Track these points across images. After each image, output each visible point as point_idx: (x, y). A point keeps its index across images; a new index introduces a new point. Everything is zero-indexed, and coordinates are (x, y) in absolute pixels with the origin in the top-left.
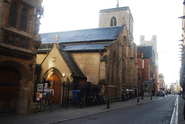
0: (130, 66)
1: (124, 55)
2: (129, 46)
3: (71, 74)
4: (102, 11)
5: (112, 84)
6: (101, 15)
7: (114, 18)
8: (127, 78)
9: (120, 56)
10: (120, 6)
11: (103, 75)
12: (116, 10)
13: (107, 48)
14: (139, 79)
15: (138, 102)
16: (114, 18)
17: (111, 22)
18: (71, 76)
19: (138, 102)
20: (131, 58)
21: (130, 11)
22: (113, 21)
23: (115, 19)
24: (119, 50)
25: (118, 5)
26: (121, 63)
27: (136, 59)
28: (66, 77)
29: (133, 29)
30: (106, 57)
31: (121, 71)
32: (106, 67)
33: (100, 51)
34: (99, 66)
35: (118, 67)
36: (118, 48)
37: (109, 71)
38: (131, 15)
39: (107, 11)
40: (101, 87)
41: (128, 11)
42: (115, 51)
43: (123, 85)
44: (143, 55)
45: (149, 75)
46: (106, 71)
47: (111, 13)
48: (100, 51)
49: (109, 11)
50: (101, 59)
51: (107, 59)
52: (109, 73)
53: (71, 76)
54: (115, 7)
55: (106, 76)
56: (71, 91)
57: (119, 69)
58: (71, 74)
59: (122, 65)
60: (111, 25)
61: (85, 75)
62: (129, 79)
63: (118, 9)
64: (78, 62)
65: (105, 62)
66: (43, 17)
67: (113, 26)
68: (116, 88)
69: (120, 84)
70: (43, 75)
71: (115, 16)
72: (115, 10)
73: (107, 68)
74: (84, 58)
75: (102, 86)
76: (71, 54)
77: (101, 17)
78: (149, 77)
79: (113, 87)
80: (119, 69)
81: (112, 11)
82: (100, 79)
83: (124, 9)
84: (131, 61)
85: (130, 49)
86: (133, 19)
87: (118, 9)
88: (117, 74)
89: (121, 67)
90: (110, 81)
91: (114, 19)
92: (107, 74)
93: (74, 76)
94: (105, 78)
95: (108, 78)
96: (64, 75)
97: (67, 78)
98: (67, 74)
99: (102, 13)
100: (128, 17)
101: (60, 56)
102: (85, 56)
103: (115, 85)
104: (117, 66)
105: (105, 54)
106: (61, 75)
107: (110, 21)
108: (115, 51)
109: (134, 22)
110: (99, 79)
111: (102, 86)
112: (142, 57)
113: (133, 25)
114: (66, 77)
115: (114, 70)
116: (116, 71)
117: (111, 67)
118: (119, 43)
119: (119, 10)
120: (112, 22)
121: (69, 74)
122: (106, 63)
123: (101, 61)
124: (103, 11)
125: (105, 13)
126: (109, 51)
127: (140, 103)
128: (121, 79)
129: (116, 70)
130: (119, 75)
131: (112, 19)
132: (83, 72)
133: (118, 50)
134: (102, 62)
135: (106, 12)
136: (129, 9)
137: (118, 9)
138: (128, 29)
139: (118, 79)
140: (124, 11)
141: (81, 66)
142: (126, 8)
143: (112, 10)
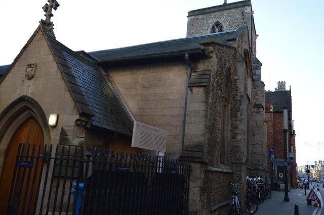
0: (253, 123)
3: (78, 117)
4: (192, 14)
5: (223, 163)
6: (191, 20)
7: (218, 25)
11: (196, 131)
13: (211, 48)
20: (258, 106)
24: (239, 74)
30: (204, 74)
31: (243, 127)
32: (206, 102)
33: (187, 55)
34: (183, 105)
35: (236, 116)
37: (216, 119)
38: (252, 17)
39: (204, 12)
40: (190, 170)
41: (248, 10)
43: (247, 168)
46: (206, 116)
48: (187, 55)
49: (207, 11)
50: (192, 80)
51: (209, 79)
53: (78, 123)
54: (222, 3)
55: (207, 135)
56: (68, 184)
57: (238, 123)
58: (78, 117)
59: (247, 111)
60: (213, 30)
62: (253, 153)
63: (227, 7)
64: (122, 93)
68: (232, 174)
69: (243, 164)
71: (221, 20)
72: (216, 9)
73: (210, 108)
74: (140, 81)
75: (193, 165)
76: (107, 72)
77: (190, 25)
79: (225, 171)
80: (238, 123)
81: (214, 12)
82: (186, 143)
83: (240, 5)
84: (257, 113)
88: (234, 136)
90: (217, 153)
91: (217, 27)
92: (211, 128)
94: (202, 139)
95: (212, 143)
96: (52, 120)
97: (63, 133)
99: (193, 17)
101: (51, 57)
102: (143, 76)
103: (227, 165)
104: (234, 115)
105: (201, 67)
106: (45, 121)
110: (183, 144)
111: (193, 165)
112: (271, 110)
113: (255, 43)
114: (59, 128)
115: (226, 123)
116: (230, 127)
118: (238, 54)
122: (207, 93)
123: (191, 86)
124: (196, 13)
125: (200, 17)
129: (230, 123)
130: (239, 137)
131: (213, 28)
134: (195, 90)
139: (235, 149)
143: (214, 10)
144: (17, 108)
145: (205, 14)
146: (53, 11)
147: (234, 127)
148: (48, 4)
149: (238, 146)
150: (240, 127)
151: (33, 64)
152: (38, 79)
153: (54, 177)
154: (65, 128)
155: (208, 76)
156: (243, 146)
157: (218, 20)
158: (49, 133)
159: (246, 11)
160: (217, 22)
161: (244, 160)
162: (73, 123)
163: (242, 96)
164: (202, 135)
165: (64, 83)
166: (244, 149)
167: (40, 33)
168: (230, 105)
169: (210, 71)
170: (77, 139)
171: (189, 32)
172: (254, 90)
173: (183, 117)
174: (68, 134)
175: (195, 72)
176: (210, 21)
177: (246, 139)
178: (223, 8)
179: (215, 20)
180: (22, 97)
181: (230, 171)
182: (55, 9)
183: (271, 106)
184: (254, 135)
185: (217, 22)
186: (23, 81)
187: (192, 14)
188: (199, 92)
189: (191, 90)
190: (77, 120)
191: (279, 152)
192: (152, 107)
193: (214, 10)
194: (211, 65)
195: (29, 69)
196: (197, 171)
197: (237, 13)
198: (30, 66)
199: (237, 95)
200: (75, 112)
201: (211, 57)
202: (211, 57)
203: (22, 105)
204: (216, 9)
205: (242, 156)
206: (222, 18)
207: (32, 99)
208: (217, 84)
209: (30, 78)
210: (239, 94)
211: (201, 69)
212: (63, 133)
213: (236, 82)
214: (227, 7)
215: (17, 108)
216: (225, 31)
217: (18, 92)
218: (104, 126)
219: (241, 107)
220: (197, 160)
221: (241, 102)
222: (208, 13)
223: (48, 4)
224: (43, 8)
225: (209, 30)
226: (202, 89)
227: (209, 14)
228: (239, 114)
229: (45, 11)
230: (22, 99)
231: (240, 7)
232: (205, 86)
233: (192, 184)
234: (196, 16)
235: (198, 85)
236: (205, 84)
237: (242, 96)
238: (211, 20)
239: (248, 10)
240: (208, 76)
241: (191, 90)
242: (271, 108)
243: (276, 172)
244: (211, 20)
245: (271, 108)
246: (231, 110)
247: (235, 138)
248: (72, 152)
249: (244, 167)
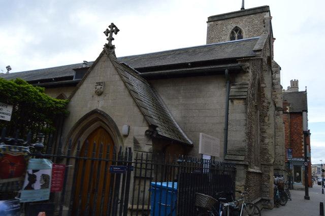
3: (147, 128)
4: (214, 20)
6: (210, 25)
7: (237, 29)
10: (246, 7)
11: (238, 137)
12: (239, 14)
13: (248, 64)
16: (237, 29)
18: (146, 135)
22: (236, 35)
23: (240, 32)
28: (131, 137)
32: (246, 112)
33: (226, 71)
34: (223, 113)
35: (264, 121)
38: (270, 21)
39: (223, 18)
40: (234, 172)
41: (266, 15)
44: (290, 108)
47: (231, 21)
48: (226, 71)
49: (227, 17)
54: (239, 9)
55: (247, 141)
56: (142, 183)
57: (265, 127)
58: (147, 128)
61: (186, 137)
70: (70, 129)
73: (249, 116)
76: (150, 84)
77: (210, 30)
79: (258, 171)
83: (259, 11)
87: (243, 13)
91: (237, 32)
92: (249, 135)
93: (155, 136)
94: (244, 145)
95: (250, 145)
97: (136, 142)
99: (212, 23)
104: (262, 121)
105: (241, 80)
109: (275, 41)
111: (237, 167)
116: (259, 132)
119: (249, 15)
121: (140, 130)
122: (246, 104)
123: (231, 99)
124: (216, 19)
125: (220, 22)
126: (250, 74)
130: (267, 141)
131: (232, 33)
132: (180, 129)
133: (263, 79)
134: (236, 102)
136: (269, 11)
137: (242, 14)
139: (264, 151)
140: (258, 15)
141: (175, 114)
142: (265, 9)
144: (90, 119)
145: (223, 19)
146: (114, 35)
147: (263, 131)
148: (109, 29)
149: (266, 149)
150: (267, 131)
151: (102, 83)
152: (107, 95)
153: (135, 178)
154: (136, 137)
155: (246, 90)
157: (238, 26)
158: (122, 141)
159: (265, 17)
160: (236, 27)
161: (272, 161)
162: (144, 133)
163: (269, 103)
164: (243, 141)
165: (132, 99)
166: (271, 152)
167: (105, 55)
168: (259, 111)
169: (248, 84)
170: (147, 147)
172: (274, 93)
173: (223, 126)
174: (140, 142)
175: (233, 85)
176: (229, 27)
177: (274, 142)
178: (242, 14)
180: (93, 111)
181: (260, 171)
182: (116, 34)
183: (287, 107)
185: (236, 27)
186: (93, 96)
187: (211, 20)
188: (238, 105)
189: (232, 102)
190: (147, 131)
191: (296, 152)
192: (195, 115)
194: (248, 78)
195: (99, 87)
196: (241, 173)
197: (256, 19)
198: (99, 84)
199: (264, 101)
200: (145, 124)
201: (248, 72)
202: (248, 72)
203: (94, 116)
204: (235, 15)
205: (270, 158)
206: (242, 23)
207: (103, 112)
208: (252, 96)
209: (99, 94)
210: (266, 101)
211: (240, 83)
212: (136, 142)
213: (263, 90)
214: (246, 13)
215: (90, 119)
217: (89, 106)
218: (164, 135)
219: (269, 113)
220: (241, 163)
221: (268, 109)
222: (228, 18)
223: (109, 29)
224: (104, 32)
225: (228, 36)
226: (242, 101)
227: (229, 20)
228: (266, 119)
229: (107, 35)
230: (95, 112)
231: (259, 13)
232: (244, 99)
233: (237, 183)
234: (216, 23)
235: (238, 97)
236: (245, 97)
237: (269, 103)
238: (231, 25)
240: (246, 90)
241: (232, 102)
242: (287, 109)
243: (293, 171)
244: (231, 25)
245: (287, 109)
246: (260, 116)
247: (262, 141)
248: (144, 157)
249: (272, 168)
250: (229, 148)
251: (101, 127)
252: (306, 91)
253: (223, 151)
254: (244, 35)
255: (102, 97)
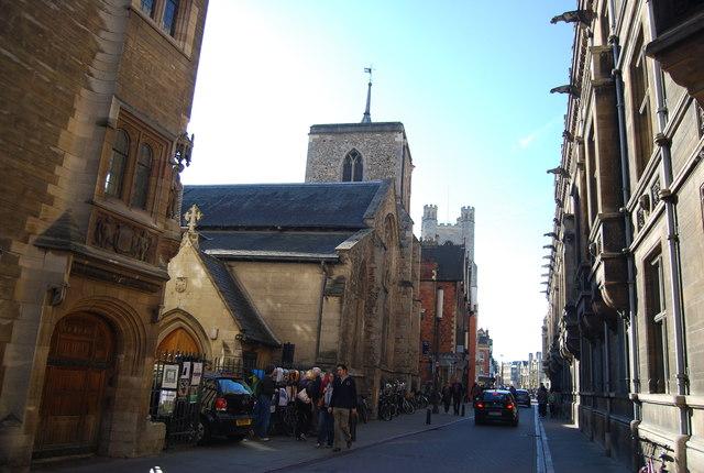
1: (386, 275)
2: (401, 246)
3: (238, 332)
4: (317, 130)
7: (354, 153)
8: (391, 346)
9: (378, 277)
10: (377, 117)
14: (425, 348)
15: (428, 422)
16: (354, 153)
17: (345, 166)
19: (428, 422)
20: (406, 284)
21: (405, 137)
23: (360, 159)
25: (367, 114)
26: (380, 301)
27: (417, 284)
29: (409, 191)
30: (340, 281)
31: (378, 325)
34: (317, 311)
36: (372, 253)
38: (406, 147)
41: (399, 138)
42: (364, 262)
45: (454, 337)
52: (346, 332)
54: (358, 119)
58: (238, 332)
60: (346, 177)
63: (369, 128)
65: (337, 299)
66: (188, 165)
67: (352, 182)
71: (360, 148)
72: (358, 129)
77: (312, 148)
78: (454, 343)
85: (402, 255)
86: (411, 160)
87: (367, 127)
89: (379, 312)
90: (349, 358)
92: (344, 336)
98: (225, 332)
99: (317, 137)
100: (399, 152)
104: (369, 311)
105: (338, 272)
107: (340, 166)
108: (364, 262)
109: (415, 170)
117: (353, 313)
120: (347, 167)
122: (341, 302)
123: (326, 293)
124: (322, 130)
125: (329, 138)
127: (431, 427)
128: (378, 350)
130: (373, 337)
131: (347, 157)
135: (330, 133)
138: (399, 193)
139: (369, 350)
141: (262, 306)
142: (396, 127)
143: (349, 129)
156: (377, 347)
171: (312, 165)
178: (363, 129)
179: (351, 147)
184: (398, 325)
188: (333, 301)
193: (349, 129)
195: (181, 283)
206: (363, 145)
216: (364, 182)
222: (340, 133)
239: (399, 138)
249: (377, 370)
250: (321, 350)
251: (181, 328)
252: (464, 245)
253: (314, 353)
254: (365, 167)
255: (185, 293)
